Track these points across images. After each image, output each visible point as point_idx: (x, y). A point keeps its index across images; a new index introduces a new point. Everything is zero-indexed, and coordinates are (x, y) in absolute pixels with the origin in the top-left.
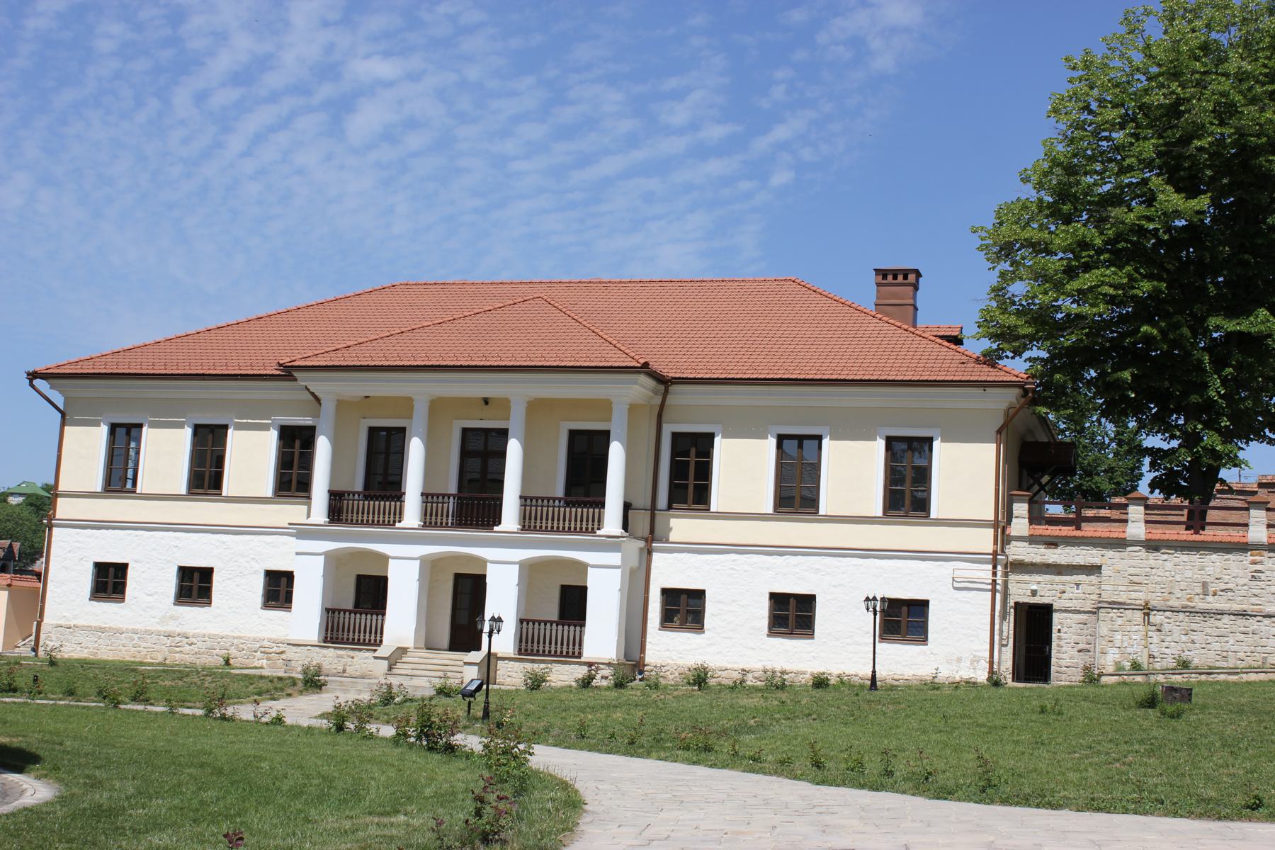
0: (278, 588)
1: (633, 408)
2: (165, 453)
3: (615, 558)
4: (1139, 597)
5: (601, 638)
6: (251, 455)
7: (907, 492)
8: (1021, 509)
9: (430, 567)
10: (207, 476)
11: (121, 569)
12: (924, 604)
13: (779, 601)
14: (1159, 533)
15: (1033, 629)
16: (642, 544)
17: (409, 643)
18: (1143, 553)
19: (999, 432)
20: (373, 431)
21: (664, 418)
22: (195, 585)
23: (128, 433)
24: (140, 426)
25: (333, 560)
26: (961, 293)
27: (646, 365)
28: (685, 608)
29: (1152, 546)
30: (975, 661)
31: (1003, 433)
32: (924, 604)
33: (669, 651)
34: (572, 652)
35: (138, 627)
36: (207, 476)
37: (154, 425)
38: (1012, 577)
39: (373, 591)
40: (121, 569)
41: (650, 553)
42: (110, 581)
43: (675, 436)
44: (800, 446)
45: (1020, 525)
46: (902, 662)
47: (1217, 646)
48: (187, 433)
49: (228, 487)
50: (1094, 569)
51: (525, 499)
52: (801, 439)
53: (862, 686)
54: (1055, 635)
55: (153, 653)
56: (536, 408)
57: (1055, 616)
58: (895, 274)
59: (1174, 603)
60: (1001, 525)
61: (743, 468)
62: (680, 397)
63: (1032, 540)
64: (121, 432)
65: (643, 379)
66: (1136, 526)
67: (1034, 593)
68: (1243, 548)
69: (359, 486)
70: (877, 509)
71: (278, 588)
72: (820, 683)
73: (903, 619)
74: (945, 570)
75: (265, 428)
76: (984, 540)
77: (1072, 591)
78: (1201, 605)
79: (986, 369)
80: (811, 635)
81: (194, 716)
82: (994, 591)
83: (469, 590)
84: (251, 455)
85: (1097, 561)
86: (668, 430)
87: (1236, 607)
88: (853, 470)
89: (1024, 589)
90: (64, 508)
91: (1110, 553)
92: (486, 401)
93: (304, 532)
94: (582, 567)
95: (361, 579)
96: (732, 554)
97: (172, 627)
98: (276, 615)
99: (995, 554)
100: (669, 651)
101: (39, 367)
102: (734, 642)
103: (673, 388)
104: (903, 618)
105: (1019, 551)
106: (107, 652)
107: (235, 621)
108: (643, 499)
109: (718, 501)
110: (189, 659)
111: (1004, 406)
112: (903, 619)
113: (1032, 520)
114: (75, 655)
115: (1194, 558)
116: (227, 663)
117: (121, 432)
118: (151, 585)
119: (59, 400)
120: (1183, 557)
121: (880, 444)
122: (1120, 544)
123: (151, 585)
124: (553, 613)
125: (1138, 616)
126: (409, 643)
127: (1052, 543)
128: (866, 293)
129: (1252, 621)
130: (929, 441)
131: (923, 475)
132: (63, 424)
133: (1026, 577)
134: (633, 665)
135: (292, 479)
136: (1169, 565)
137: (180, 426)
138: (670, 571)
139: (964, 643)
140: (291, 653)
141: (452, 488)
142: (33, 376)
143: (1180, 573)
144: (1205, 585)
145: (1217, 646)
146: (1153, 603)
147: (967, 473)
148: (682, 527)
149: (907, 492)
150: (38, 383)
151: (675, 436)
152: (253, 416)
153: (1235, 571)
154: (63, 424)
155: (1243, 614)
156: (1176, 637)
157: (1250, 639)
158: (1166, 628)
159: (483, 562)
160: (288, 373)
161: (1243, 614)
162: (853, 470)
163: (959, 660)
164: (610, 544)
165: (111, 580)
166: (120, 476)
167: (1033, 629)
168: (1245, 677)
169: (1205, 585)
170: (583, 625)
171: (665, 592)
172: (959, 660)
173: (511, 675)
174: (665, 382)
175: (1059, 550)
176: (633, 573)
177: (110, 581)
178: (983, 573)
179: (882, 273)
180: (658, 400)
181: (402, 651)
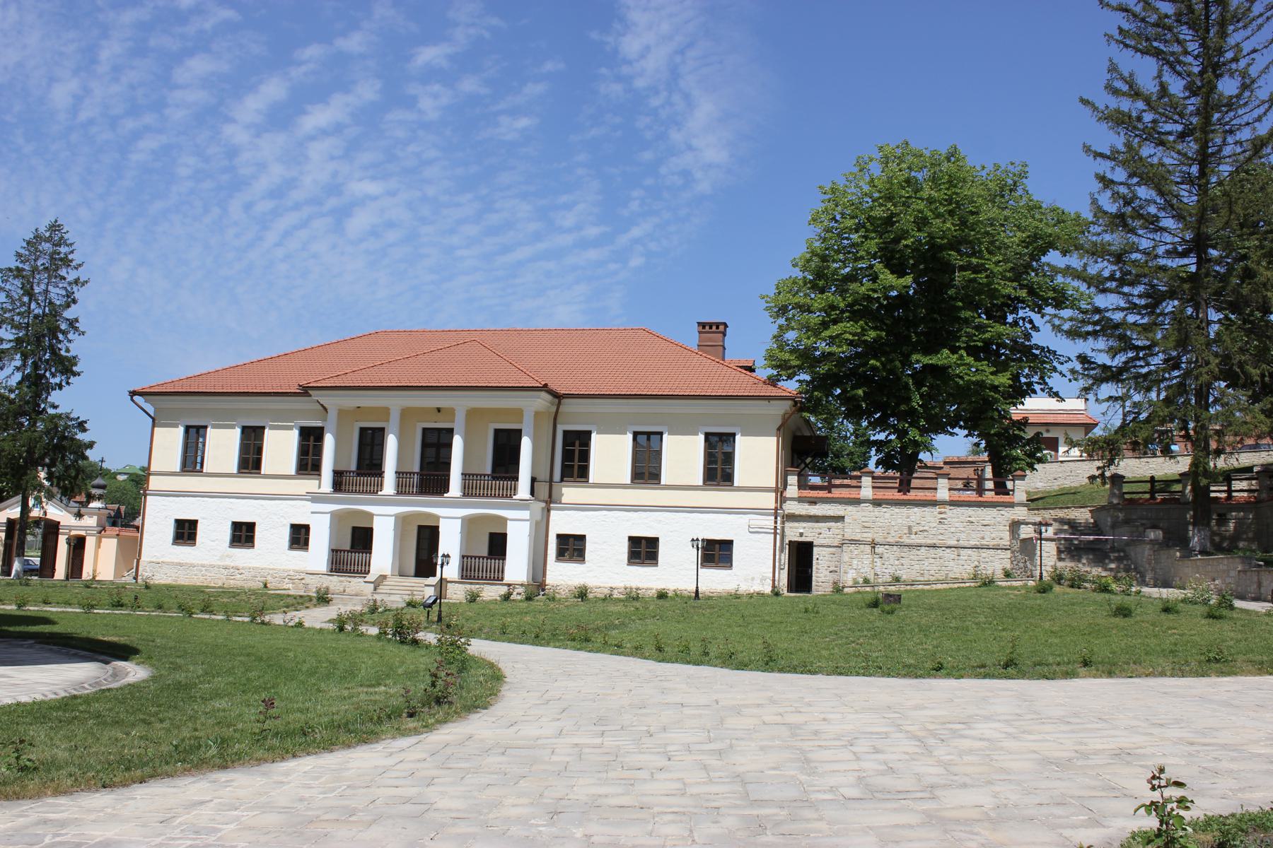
0: (299, 536)
1: (537, 414)
2: (223, 445)
3: (525, 514)
4: (868, 536)
5: (516, 568)
6: (281, 447)
7: (719, 469)
8: (793, 480)
9: (402, 521)
10: (251, 461)
11: (193, 524)
12: (730, 543)
13: (634, 541)
14: (882, 494)
15: (801, 556)
16: (543, 505)
17: (388, 572)
18: (871, 507)
19: (779, 429)
20: (363, 430)
21: (559, 419)
22: (243, 534)
23: (198, 432)
24: (206, 427)
25: (336, 518)
26: (754, 337)
27: (546, 385)
28: (572, 547)
29: (877, 503)
30: (763, 579)
31: (781, 430)
32: (730, 543)
33: (562, 575)
34: (498, 577)
35: (205, 562)
36: (251, 461)
37: (215, 427)
38: (788, 525)
39: (362, 538)
40: (193, 524)
41: (549, 511)
42: (186, 531)
43: (566, 433)
44: (649, 439)
45: (792, 491)
46: (715, 581)
47: (917, 567)
48: (238, 431)
49: (265, 469)
50: (840, 519)
51: (465, 476)
52: (649, 434)
53: (689, 597)
54: (814, 562)
55: (214, 579)
56: (472, 414)
57: (815, 549)
59: (890, 540)
60: (780, 490)
61: (611, 454)
62: (569, 406)
63: (800, 500)
64: (193, 431)
65: (544, 395)
66: (867, 489)
67: (801, 535)
68: (934, 503)
69: (353, 467)
70: (699, 480)
71: (299, 536)
72: (662, 595)
73: (716, 552)
74: (744, 519)
75: (290, 428)
76: (769, 500)
77: (826, 533)
78: (906, 541)
79: (771, 388)
80: (656, 564)
81: (243, 622)
82: (775, 534)
83: (428, 537)
84: (281, 447)
85: (841, 513)
86: (560, 429)
87: (929, 542)
88: (683, 455)
89: (795, 532)
90: (154, 483)
91: (850, 508)
92: (439, 410)
93: (316, 498)
94: (504, 521)
95: (355, 529)
96: (603, 510)
97: (228, 562)
98: (298, 554)
99: (776, 509)
100: (562, 575)
101: (137, 388)
102: (606, 570)
103: (564, 401)
104: (716, 553)
105: (792, 507)
106: (184, 579)
107: (270, 558)
108: (544, 475)
109: (593, 476)
110: (239, 584)
111: (782, 412)
112: (716, 552)
113: (800, 487)
114: (163, 582)
115: (904, 511)
116: (265, 586)
117: (193, 431)
118: (215, 534)
119: (151, 410)
120: (896, 510)
121: (701, 437)
122: (857, 502)
123: (215, 534)
124: (484, 551)
125: (868, 548)
126: (388, 572)
127: (813, 502)
128: (692, 338)
129: (939, 550)
130: (734, 435)
131: (729, 458)
132: (154, 426)
133: (796, 524)
134: (537, 585)
135: (308, 463)
136: (887, 515)
137: (232, 427)
138: (562, 522)
139: (756, 568)
140: (308, 579)
141: (416, 469)
142: (133, 394)
143: (894, 520)
144: (910, 528)
145: (917, 567)
146: (877, 540)
147: (758, 456)
148: (570, 493)
149: (719, 469)
150: (136, 398)
151: (566, 433)
152: (282, 419)
153: (929, 518)
154: (154, 426)
155: (934, 546)
156: (891, 562)
157: (938, 562)
158: (886, 556)
159: (437, 518)
160: (305, 391)
161: (934, 546)
162: (683, 455)
163: (753, 579)
164: (522, 505)
165: (186, 531)
166: (192, 461)
167: (801, 556)
168: (934, 587)
169: (910, 528)
170: (504, 559)
171: (559, 536)
172: (753, 579)
173: (457, 593)
174: (559, 397)
175: (817, 506)
176: (537, 524)
177: (186, 531)
178: (769, 522)
179: (703, 325)
180: (554, 409)
181: (384, 577)
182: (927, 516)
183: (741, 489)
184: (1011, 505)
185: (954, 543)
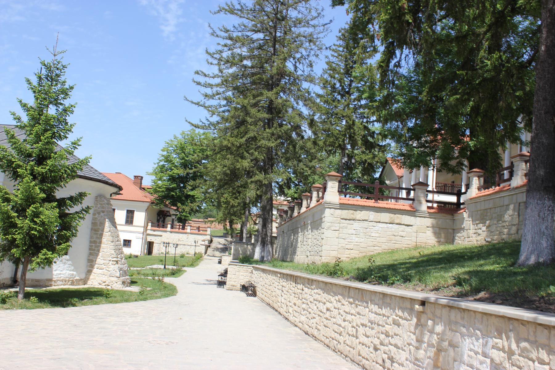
7: (129, 220)
8: (150, 224)
15: (150, 245)
29: (171, 232)
31: (147, 210)
45: (149, 227)
50: (161, 236)
58: (137, 177)
60: (146, 228)
63: (151, 230)
68: (186, 233)
76: (142, 230)
89: (149, 239)
105: (149, 232)
112: (127, 243)
122: (166, 231)
127: (154, 231)
131: (132, 217)
147: (140, 217)
149: (129, 220)
179: (135, 177)
182: (185, 236)
183: (135, 226)
184: (206, 235)
185: (190, 244)
